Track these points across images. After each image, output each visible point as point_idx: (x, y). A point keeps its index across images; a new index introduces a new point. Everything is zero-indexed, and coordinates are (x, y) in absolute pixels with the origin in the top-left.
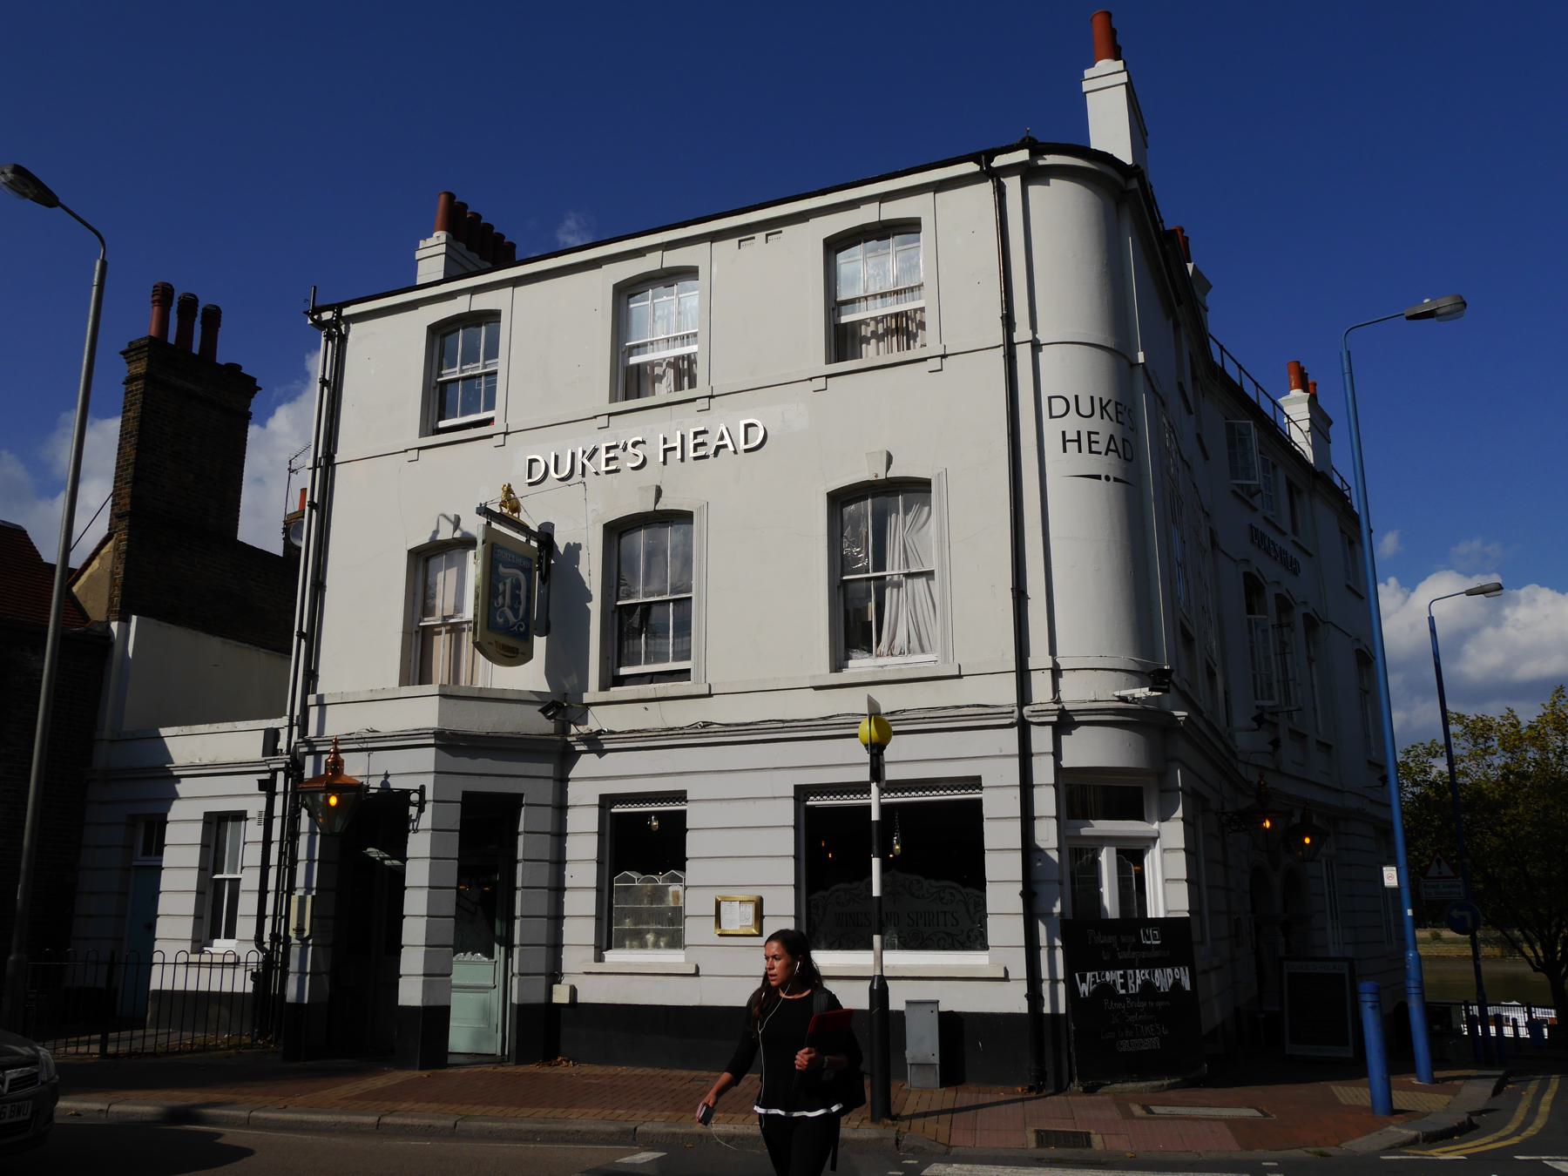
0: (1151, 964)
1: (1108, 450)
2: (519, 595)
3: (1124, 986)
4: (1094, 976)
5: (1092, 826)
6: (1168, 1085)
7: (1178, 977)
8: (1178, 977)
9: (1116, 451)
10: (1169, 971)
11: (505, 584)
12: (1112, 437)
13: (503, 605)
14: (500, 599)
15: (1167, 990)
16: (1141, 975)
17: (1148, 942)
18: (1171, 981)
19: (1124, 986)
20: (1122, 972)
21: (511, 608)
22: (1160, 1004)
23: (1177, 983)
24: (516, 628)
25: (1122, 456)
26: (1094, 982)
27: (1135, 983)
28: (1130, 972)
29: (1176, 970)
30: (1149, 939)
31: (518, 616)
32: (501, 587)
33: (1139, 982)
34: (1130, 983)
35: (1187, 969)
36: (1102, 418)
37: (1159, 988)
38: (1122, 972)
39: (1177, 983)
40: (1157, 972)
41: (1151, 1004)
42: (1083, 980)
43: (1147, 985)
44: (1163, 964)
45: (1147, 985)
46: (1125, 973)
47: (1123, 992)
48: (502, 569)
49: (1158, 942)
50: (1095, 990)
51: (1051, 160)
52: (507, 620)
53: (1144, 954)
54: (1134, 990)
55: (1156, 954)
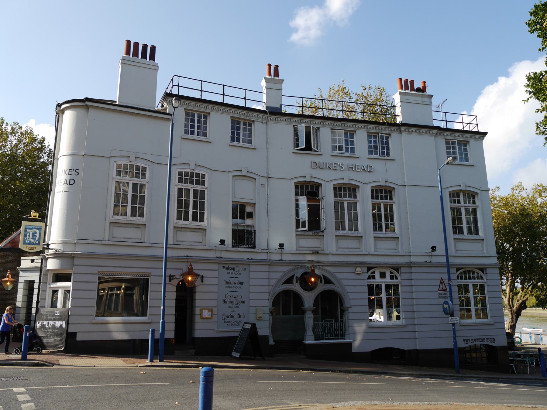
0: (55, 320)
1: (64, 183)
2: (36, 235)
3: (48, 325)
4: (41, 323)
5: (57, 284)
6: (51, 351)
7: (62, 324)
8: (62, 324)
9: (67, 183)
10: (60, 322)
11: (30, 233)
12: (66, 180)
13: (29, 238)
14: (28, 237)
15: (58, 327)
16: (52, 323)
17: (56, 314)
18: (60, 325)
19: (48, 325)
20: (48, 322)
21: (33, 238)
22: (56, 331)
23: (61, 326)
24: (34, 243)
25: (68, 183)
26: (41, 324)
27: (50, 325)
28: (50, 322)
29: (62, 322)
30: (57, 313)
31: (35, 240)
32: (28, 234)
33: (52, 325)
34: (49, 324)
35: (65, 322)
36: (64, 175)
37: (56, 327)
38: (48, 322)
39: (61, 326)
40: (57, 322)
41: (53, 330)
42: (39, 323)
43: (54, 326)
44: (59, 320)
45: (54, 326)
46: (49, 322)
47: (47, 327)
48: (28, 230)
49: (59, 315)
50: (41, 326)
51: (63, 106)
52: (30, 241)
53: (54, 317)
54: (50, 326)
55: (58, 318)
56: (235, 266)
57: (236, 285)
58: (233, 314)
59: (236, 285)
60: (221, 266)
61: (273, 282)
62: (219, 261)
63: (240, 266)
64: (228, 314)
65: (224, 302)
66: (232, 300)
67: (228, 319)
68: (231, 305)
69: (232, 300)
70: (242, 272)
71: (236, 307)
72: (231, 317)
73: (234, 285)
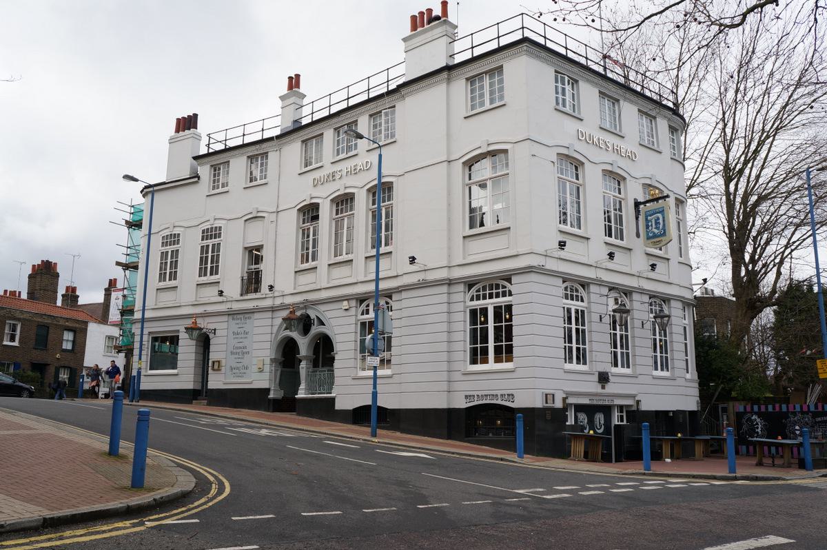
56: (242, 316)
57: (243, 336)
58: (239, 365)
59: (243, 336)
60: (231, 317)
61: (275, 329)
62: (231, 314)
63: (247, 316)
64: (234, 365)
65: (232, 353)
66: (238, 351)
67: (234, 371)
68: (237, 356)
69: (238, 351)
70: (248, 321)
71: (241, 358)
72: (238, 368)
73: (240, 336)
